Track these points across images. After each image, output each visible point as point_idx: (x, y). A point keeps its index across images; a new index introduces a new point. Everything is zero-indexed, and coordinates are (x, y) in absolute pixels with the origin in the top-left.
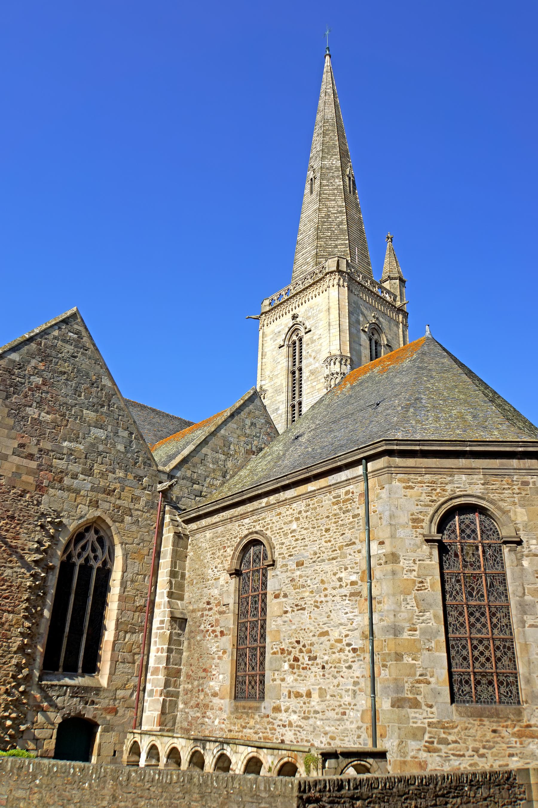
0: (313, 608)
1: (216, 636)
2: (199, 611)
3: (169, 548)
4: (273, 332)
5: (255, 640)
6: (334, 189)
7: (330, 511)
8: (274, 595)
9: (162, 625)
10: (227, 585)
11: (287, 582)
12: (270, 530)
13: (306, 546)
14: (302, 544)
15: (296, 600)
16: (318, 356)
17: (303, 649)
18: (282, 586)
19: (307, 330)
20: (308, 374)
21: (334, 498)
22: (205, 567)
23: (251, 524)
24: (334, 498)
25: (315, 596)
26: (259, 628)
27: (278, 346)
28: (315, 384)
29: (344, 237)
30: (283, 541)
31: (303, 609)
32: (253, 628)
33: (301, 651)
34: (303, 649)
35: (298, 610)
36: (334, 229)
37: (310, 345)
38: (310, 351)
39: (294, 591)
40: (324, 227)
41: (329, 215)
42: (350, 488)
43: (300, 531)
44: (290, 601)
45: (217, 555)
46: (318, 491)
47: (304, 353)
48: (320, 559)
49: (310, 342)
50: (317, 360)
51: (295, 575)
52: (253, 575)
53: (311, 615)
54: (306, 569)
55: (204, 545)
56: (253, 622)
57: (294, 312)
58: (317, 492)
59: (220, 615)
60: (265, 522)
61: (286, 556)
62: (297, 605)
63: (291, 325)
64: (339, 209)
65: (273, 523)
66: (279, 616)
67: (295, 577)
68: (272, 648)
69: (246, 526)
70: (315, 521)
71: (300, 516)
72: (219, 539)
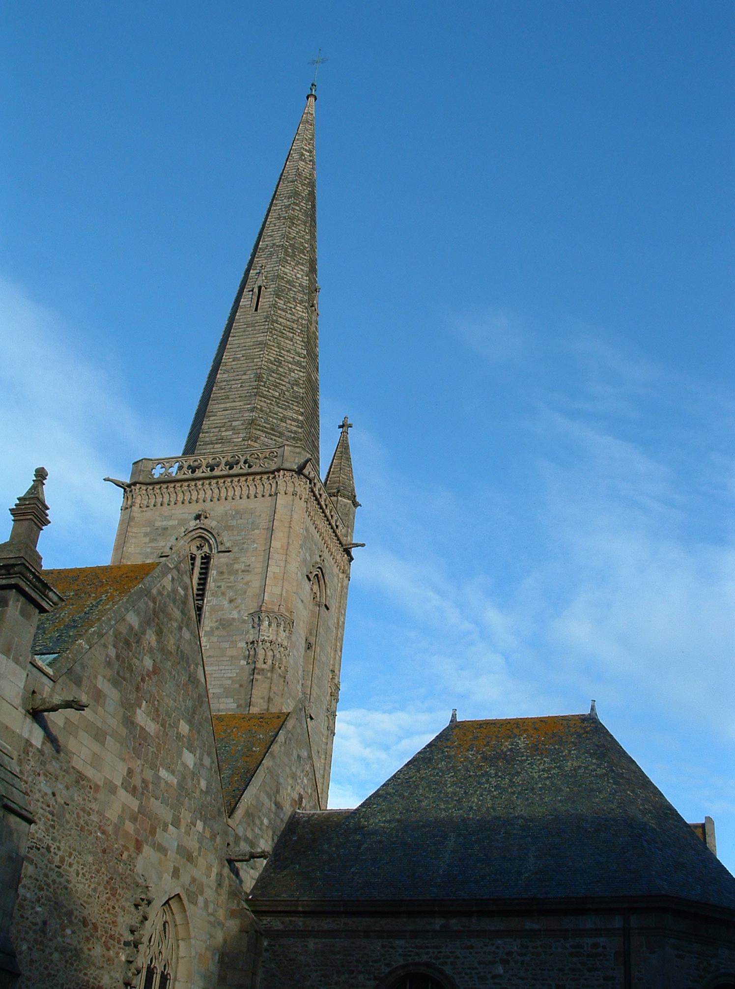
4: (150, 523)
20: (214, 625)
21: (571, 946)
24: (571, 946)
27: (160, 552)
28: (225, 645)
29: (297, 409)
36: (284, 388)
40: (270, 378)
41: (279, 363)
42: (601, 940)
47: (211, 584)
50: (236, 607)
64: (298, 358)
69: (400, 950)
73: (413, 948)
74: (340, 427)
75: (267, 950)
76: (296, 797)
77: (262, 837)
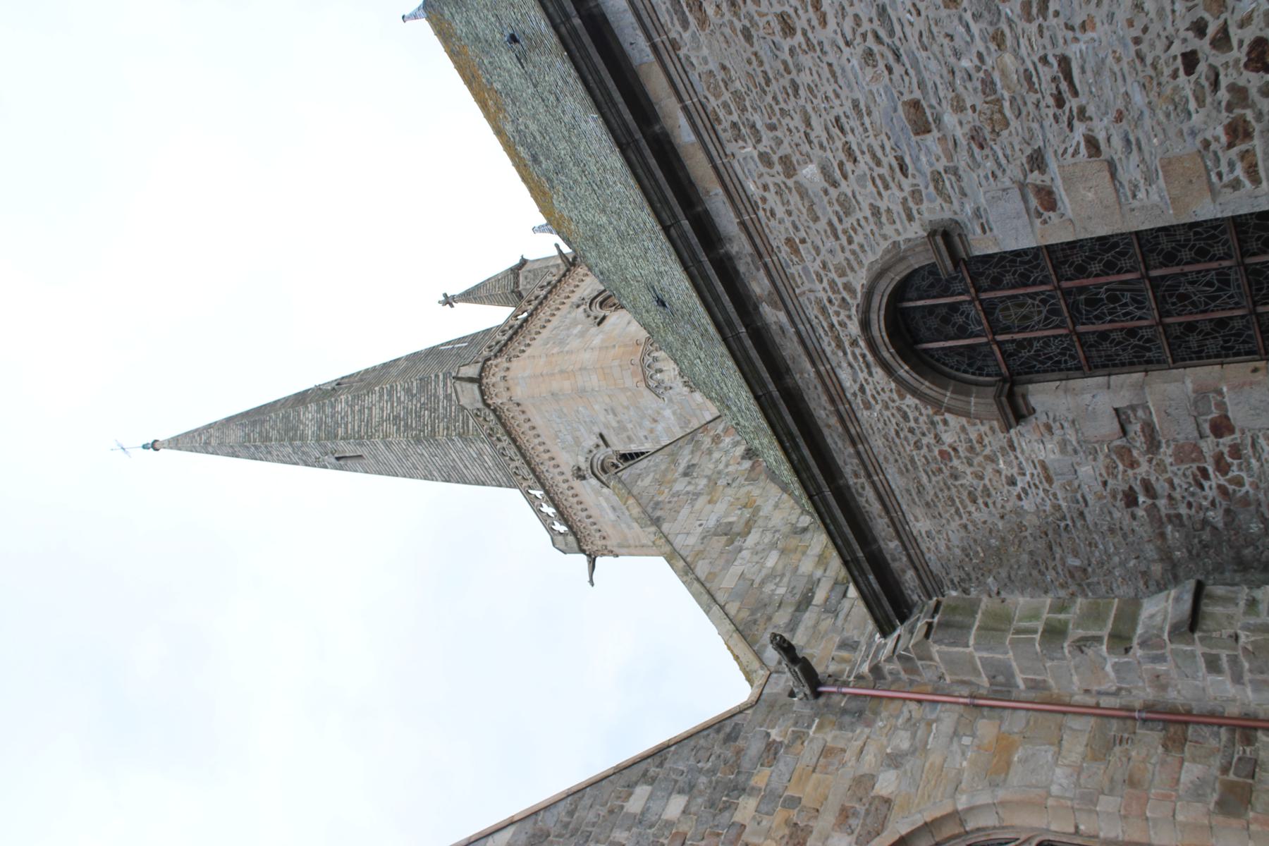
0: (1052, 21)
1: (1236, 451)
2: (1162, 535)
3: (977, 655)
5: (1224, 279)
6: (353, 412)
7: (727, 31)
8: (1046, 215)
9: (1224, 659)
10: (1056, 426)
11: (990, 164)
12: (851, 277)
13: (856, 105)
14: (854, 123)
15: (1044, 111)
16: (650, 412)
17: (1211, 30)
18: (1008, 183)
19: (601, 443)
21: (685, 25)
22: (1021, 527)
23: (850, 356)
24: (685, 25)
25: (1010, 22)
26: (1176, 270)
30: (868, 213)
31: (1064, 62)
32: (1183, 297)
33: (1222, 41)
34: (1211, 30)
35: (1075, 93)
36: (419, 405)
37: (630, 433)
38: (641, 434)
39: (1014, 123)
41: (395, 418)
43: (821, 146)
44: (1051, 136)
45: (975, 482)
46: (685, 97)
48: (883, 33)
49: (624, 435)
50: (659, 413)
51: (959, 133)
52: (1007, 330)
53: (1077, 22)
54: (930, 85)
55: (955, 540)
56: (1160, 301)
57: (569, 475)
58: (688, 102)
59: (1159, 446)
60: (830, 301)
61: (907, 184)
62: (1060, 102)
63: (594, 481)
65: (824, 266)
66: (1113, 175)
67: (967, 128)
68: (1236, 185)
70: (775, 86)
71: (775, 158)
72: (924, 479)
73: (845, 354)
74: (452, 306)
75: (966, 591)
76: (747, 464)
77: (797, 568)
